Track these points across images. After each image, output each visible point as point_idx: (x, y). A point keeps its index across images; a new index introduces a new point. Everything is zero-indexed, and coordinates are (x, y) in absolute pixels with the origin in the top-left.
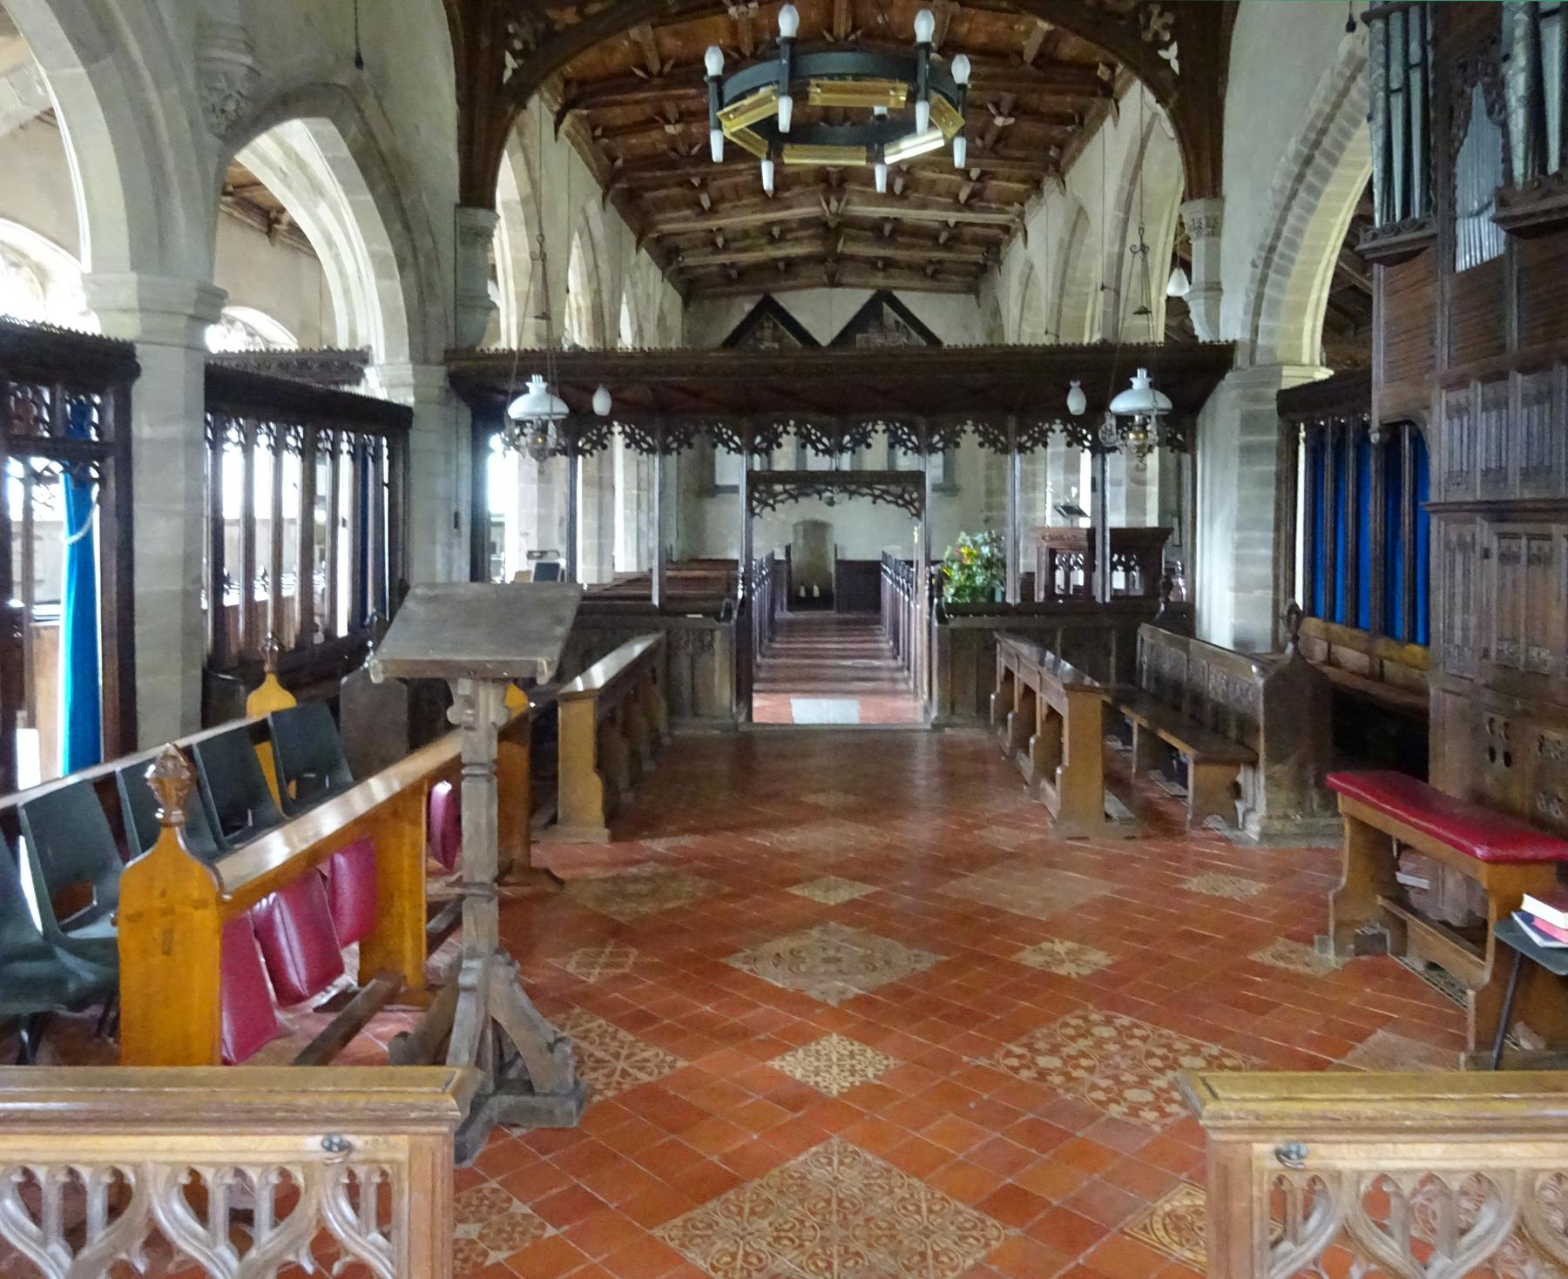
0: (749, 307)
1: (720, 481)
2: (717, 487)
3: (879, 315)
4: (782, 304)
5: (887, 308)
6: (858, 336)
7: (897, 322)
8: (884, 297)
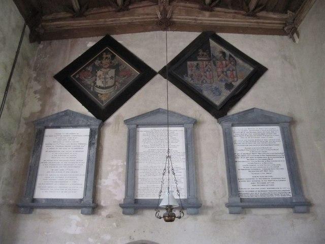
0: (90, 44)
1: (41, 193)
2: (34, 200)
3: (207, 48)
4: (119, 42)
5: (213, 43)
6: (189, 63)
7: (224, 54)
8: (209, 35)
